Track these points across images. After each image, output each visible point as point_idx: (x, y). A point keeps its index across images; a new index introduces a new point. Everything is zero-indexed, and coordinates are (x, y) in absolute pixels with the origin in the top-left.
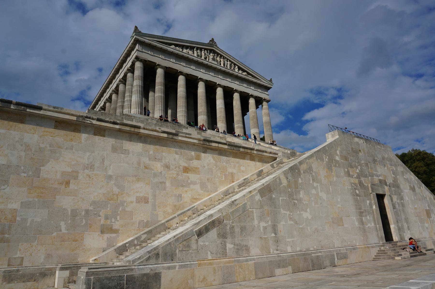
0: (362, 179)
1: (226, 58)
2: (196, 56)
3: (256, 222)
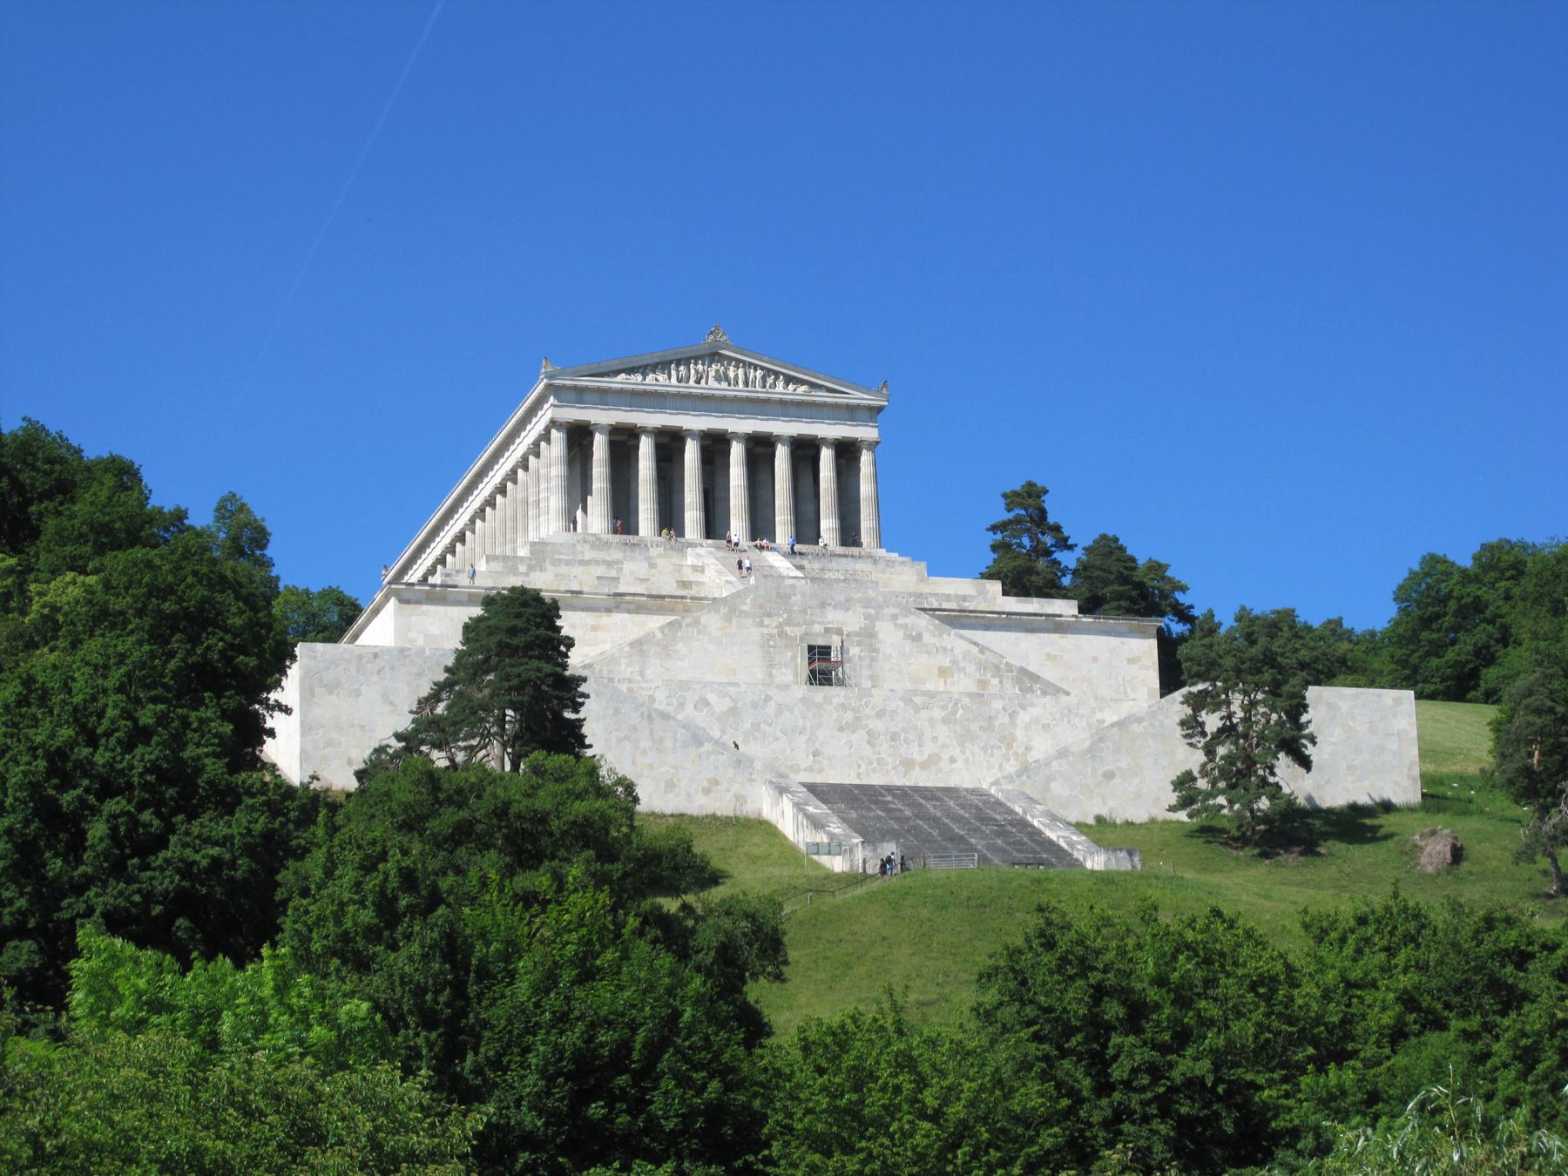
0: (788, 629)
1: (750, 364)
2: (676, 383)
3: (623, 667)
